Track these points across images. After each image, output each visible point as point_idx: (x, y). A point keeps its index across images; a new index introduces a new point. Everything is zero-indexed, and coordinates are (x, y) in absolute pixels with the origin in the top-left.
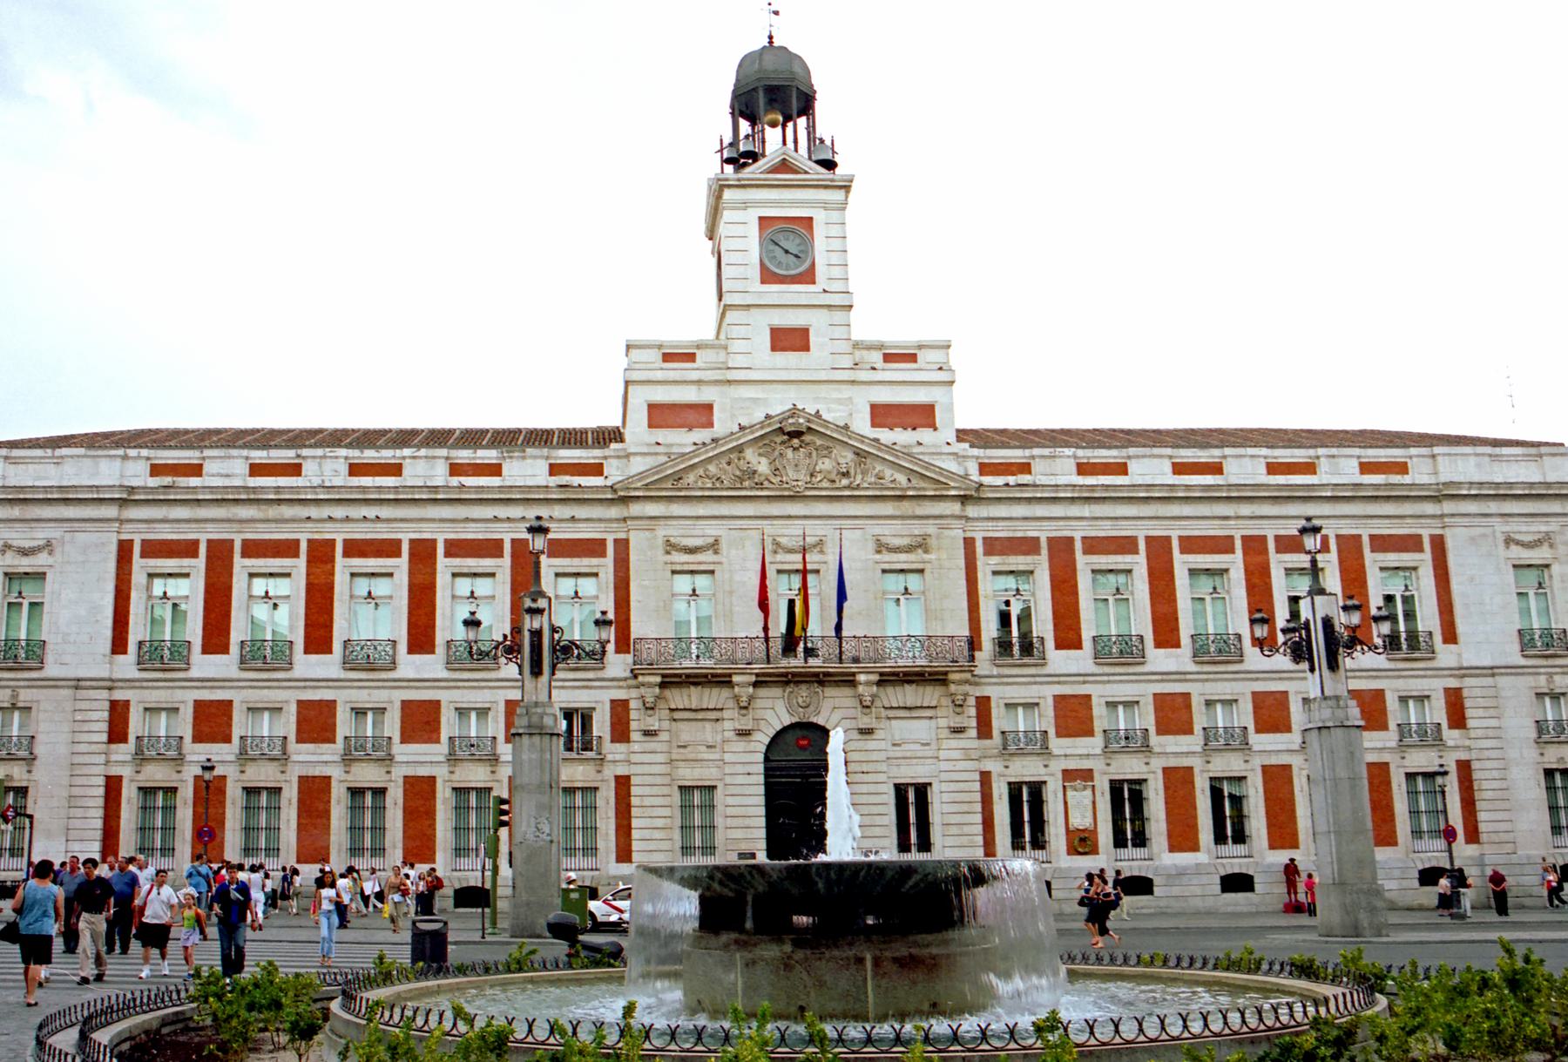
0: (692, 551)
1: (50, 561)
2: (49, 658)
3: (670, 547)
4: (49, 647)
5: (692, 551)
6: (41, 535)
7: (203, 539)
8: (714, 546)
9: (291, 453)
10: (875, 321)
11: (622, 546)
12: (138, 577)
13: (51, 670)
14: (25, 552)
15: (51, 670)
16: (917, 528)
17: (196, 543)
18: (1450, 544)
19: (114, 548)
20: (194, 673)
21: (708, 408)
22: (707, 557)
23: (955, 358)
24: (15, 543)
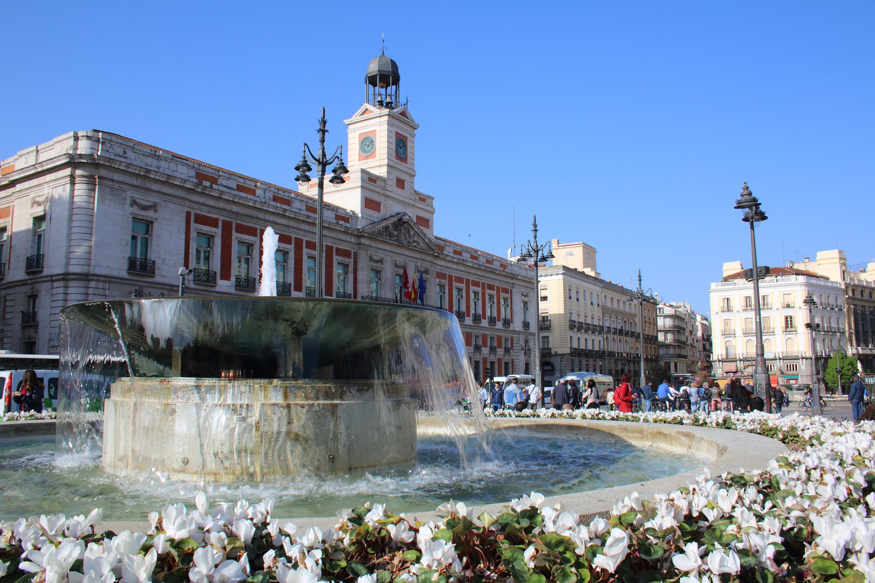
0: (377, 262)
1: (156, 216)
2: (157, 272)
3: (371, 259)
4: (156, 265)
5: (377, 262)
6: (152, 200)
7: (221, 218)
8: (381, 261)
9: (253, 184)
10: (421, 185)
11: (356, 254)
12: (193, 234)
13: (158, 279)
14: (145, 208)
15: (158, 279)
16: (428, 265)
17: (218, 219)
18: (514, 292)
19: (184, 215)
20: (217, 289)
21: (379, 204)
22: (379, 265)
23: (435, 204)
24: (138, 201)
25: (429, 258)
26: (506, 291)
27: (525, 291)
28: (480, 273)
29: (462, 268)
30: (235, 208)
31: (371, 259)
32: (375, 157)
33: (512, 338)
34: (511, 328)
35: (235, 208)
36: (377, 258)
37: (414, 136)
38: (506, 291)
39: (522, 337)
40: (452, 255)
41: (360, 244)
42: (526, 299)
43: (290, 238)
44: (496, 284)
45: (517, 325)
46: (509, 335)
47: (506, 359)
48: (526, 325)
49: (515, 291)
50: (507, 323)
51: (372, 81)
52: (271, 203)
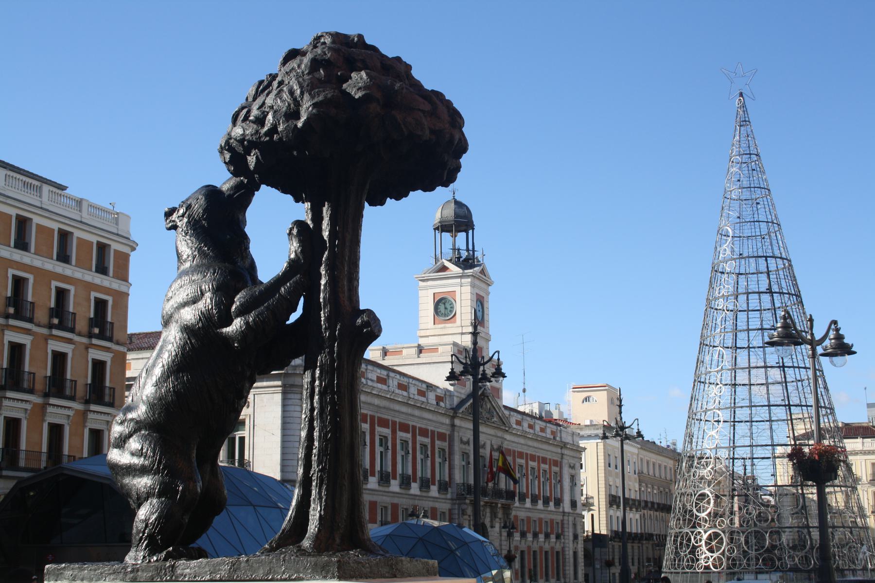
25: (500, 434)
26: (556, 463)
27: (572, 461)
28: (536, 444)
29: (522, 441)
30: (376, 401)
31: (462, 442)
32: (455, 322)
33: (562, 521)
34: (561, 510)
35: (376, 401)
36: (465, 439)
37: (488, 294)
38: (556, 463)
39: (571, 519)
40: (514, 426)
41: (453, 426)
42: (573, 472)
43: (408, 425)
44: (549, 456)
45: (566, 506)
46: (559, 518)
47: (558, 547)
48: (574, 504)
49: (565, 461)
50: (558, 502)
51: (444, 227)
52: (397, 391)
